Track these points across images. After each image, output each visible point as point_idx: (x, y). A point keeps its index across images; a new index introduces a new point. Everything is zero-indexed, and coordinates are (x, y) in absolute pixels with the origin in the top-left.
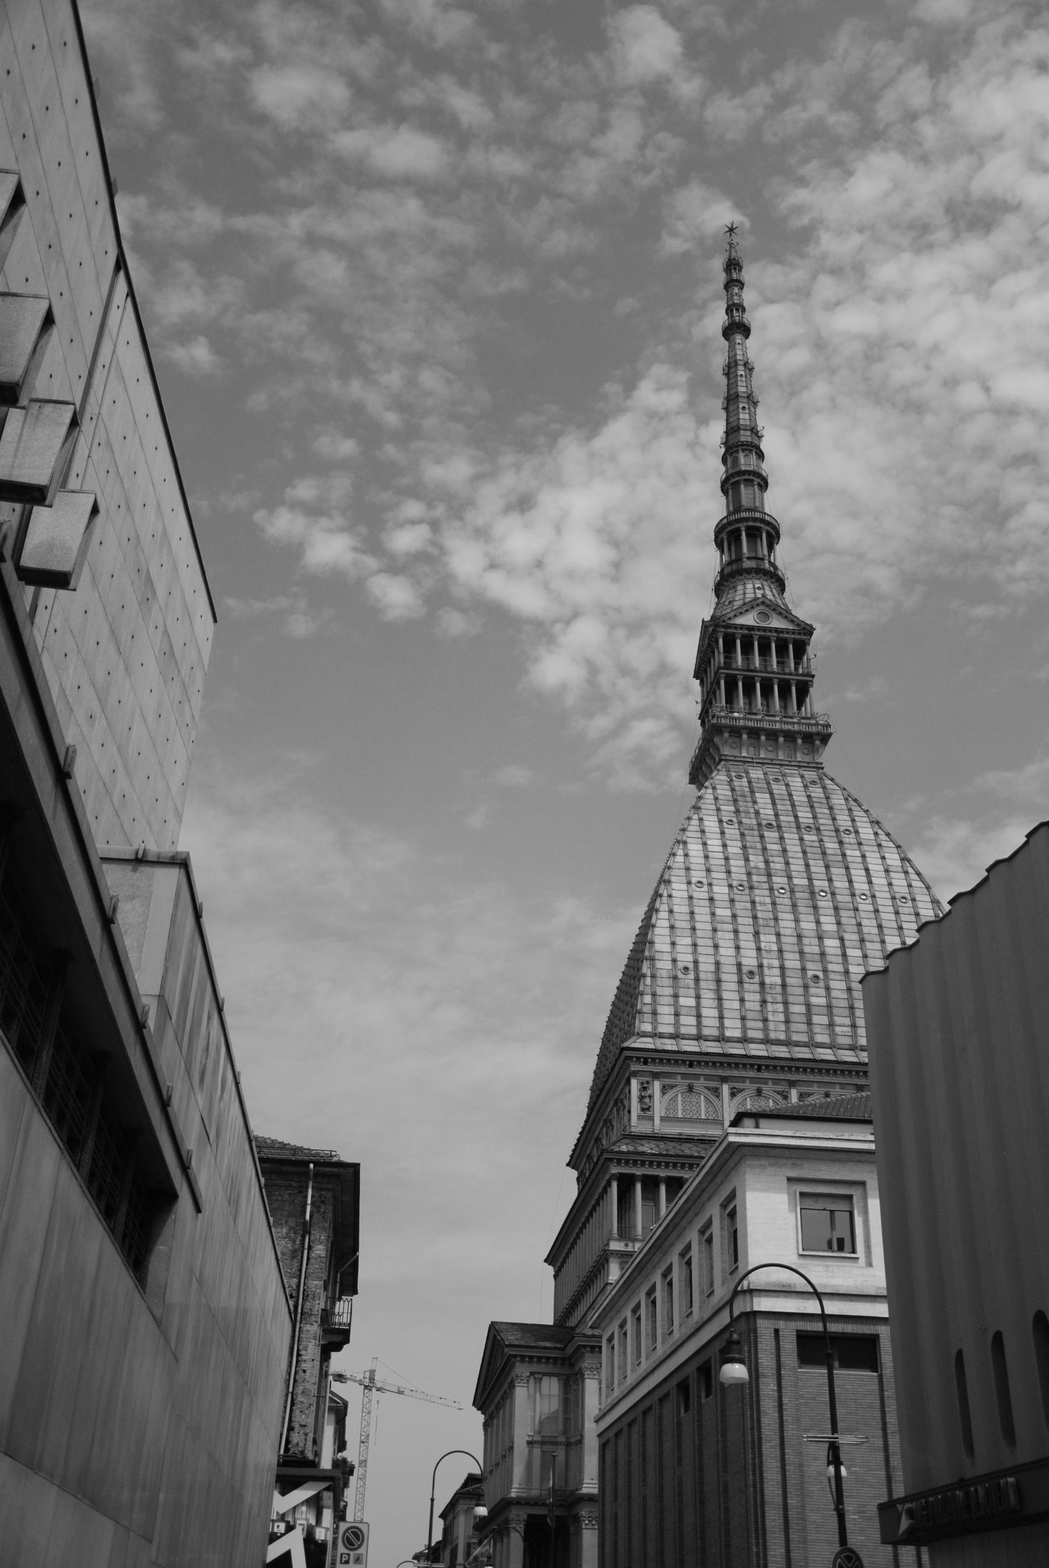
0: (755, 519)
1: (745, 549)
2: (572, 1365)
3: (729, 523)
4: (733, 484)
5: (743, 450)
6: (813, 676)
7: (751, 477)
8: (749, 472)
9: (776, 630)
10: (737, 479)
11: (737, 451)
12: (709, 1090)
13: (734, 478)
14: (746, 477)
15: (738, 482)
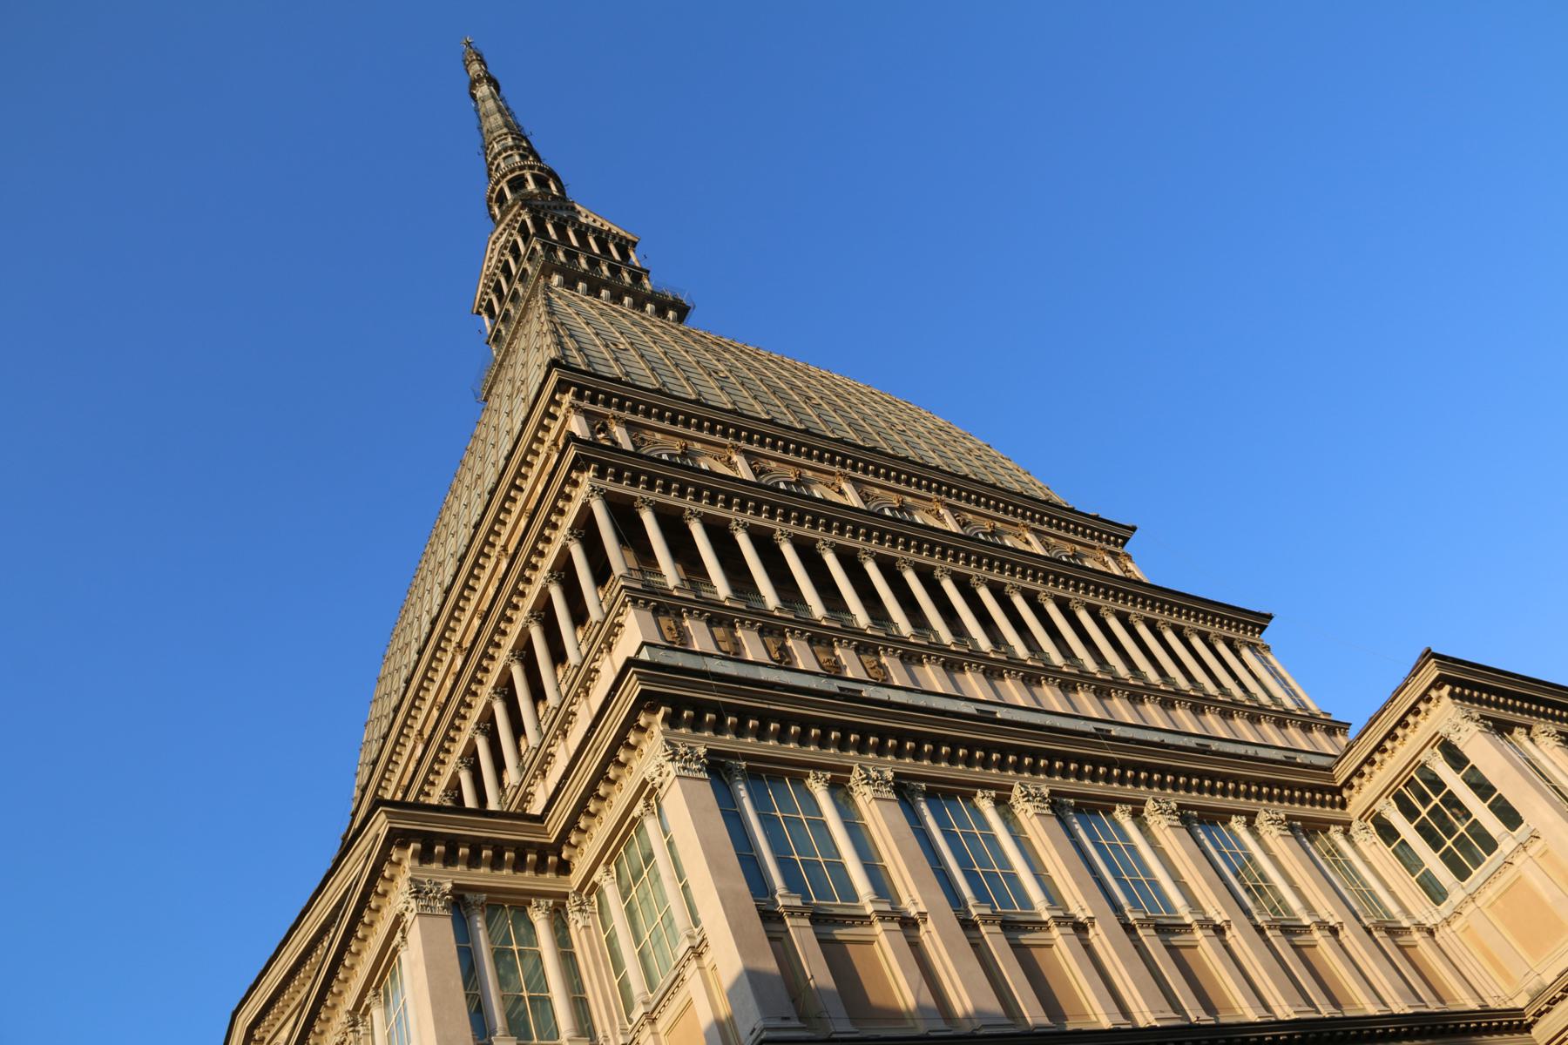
0: (541, 169)
1: (531, 186)
2: (564, 868)
3: (512, 171)
4: (505, 158)
5: (513, 138)
6: (648, 272)
7: (526, 153)
8: (524, 149)
9: (595, 230)
10: (510, 152)
11: (506, 139)
12: (715, 459)
13: (506, 151)
14: (521, 152)
15: (511, 155)
